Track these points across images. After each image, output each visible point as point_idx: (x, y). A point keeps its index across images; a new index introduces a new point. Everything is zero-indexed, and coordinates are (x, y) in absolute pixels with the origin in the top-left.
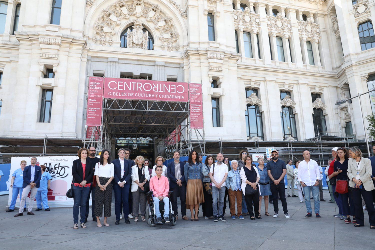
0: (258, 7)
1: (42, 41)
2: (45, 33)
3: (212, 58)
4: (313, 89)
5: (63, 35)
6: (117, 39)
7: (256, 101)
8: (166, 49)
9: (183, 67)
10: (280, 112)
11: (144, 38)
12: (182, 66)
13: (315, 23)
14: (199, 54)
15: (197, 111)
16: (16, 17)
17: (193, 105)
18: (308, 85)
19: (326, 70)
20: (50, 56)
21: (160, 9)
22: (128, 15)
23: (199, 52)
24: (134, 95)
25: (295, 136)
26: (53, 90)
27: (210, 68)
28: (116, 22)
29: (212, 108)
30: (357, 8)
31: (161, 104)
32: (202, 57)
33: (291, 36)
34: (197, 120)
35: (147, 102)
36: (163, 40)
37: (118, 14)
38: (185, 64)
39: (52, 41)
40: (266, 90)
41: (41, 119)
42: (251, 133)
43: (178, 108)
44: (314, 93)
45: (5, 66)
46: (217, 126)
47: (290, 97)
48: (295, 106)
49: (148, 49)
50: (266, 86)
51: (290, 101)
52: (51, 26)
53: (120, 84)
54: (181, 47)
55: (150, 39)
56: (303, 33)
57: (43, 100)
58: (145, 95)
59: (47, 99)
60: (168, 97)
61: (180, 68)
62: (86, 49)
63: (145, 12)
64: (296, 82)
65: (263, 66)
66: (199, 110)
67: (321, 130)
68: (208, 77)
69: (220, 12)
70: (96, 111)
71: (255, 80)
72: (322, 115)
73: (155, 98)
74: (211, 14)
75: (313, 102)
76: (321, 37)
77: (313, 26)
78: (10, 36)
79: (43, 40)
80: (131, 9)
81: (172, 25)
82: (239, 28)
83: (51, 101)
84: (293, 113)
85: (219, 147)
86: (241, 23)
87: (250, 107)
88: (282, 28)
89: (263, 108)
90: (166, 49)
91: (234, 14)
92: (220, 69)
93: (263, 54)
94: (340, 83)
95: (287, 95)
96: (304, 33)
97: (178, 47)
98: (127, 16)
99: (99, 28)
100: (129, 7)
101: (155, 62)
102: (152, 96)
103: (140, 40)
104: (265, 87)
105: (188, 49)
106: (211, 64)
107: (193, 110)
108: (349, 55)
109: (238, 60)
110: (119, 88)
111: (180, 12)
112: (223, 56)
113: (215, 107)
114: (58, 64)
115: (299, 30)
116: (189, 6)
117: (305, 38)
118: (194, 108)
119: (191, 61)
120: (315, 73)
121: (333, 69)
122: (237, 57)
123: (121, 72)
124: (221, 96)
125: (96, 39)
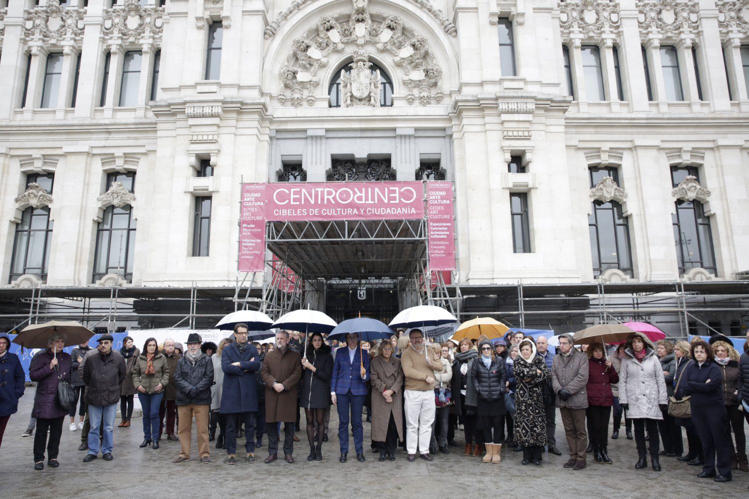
2: (195, 99)
3: (508, 112)
6: (322, 92)
8: (417, 102)
9: (451, 136)
10: (672, 214)
11: (373, 84)
15: (444, 237)
16: (155, 72)
17: (435, 224)
20: (205, 138)
21: (401, 23)
22: (342, 43)
23: (482, 102)
24: (320, 212)
25: (712, 265)
27: (505, 133)
28: (319, 60)
29: (513, 215)
31: (372, 225)
32: (486, 112)
33: (700, 41)
34: (443, 254)
35: (346, 223)
36: (410, 86)
37: (323, 45)
38: (454, 129)
39: (207, 111)
40: (637, 168)
43: (406, 232)
46: (525, 251)
47: (698, 180)
48: (708, 199)
49: (382, 106)
51: (696, 188)
52: (205, 84)
53: (295, 193)
55: (387, 85)
58: (341, 211)
60: (383, 212)
61: (444, 137)
63: (374, 33)
64: (710, 145)
65: (629, 116)
66: (446, 233)
69: (523, 15)
70: (254, 244)
73: (360, 215)
74: (506, 20)
79: (192, 112)
80: (347, 32)
82: (571, 40)
83: (209, 218)
84: (706, 215)
85: (518, 298)
86: (576, 28)
87: (602, 206)
88: (675, 25)
89: (631, 207)
90: (417, 102)
91: (559, 12)
92: (526, 134)
93: (629, 89)
95: (689, 174)
97: (441, 95)
98: (340, 46)
101: (394, 130)
102: (352, 212)
103: (365, 90)
105: (459, 98)
107: (434, 235)
110: (293, 202)
112: (531, 106)
113: (519, 211)
114: (219, 151)
118: (438, 231)
119: (465, 121)
123: (332, 155)
124: (530, 189)
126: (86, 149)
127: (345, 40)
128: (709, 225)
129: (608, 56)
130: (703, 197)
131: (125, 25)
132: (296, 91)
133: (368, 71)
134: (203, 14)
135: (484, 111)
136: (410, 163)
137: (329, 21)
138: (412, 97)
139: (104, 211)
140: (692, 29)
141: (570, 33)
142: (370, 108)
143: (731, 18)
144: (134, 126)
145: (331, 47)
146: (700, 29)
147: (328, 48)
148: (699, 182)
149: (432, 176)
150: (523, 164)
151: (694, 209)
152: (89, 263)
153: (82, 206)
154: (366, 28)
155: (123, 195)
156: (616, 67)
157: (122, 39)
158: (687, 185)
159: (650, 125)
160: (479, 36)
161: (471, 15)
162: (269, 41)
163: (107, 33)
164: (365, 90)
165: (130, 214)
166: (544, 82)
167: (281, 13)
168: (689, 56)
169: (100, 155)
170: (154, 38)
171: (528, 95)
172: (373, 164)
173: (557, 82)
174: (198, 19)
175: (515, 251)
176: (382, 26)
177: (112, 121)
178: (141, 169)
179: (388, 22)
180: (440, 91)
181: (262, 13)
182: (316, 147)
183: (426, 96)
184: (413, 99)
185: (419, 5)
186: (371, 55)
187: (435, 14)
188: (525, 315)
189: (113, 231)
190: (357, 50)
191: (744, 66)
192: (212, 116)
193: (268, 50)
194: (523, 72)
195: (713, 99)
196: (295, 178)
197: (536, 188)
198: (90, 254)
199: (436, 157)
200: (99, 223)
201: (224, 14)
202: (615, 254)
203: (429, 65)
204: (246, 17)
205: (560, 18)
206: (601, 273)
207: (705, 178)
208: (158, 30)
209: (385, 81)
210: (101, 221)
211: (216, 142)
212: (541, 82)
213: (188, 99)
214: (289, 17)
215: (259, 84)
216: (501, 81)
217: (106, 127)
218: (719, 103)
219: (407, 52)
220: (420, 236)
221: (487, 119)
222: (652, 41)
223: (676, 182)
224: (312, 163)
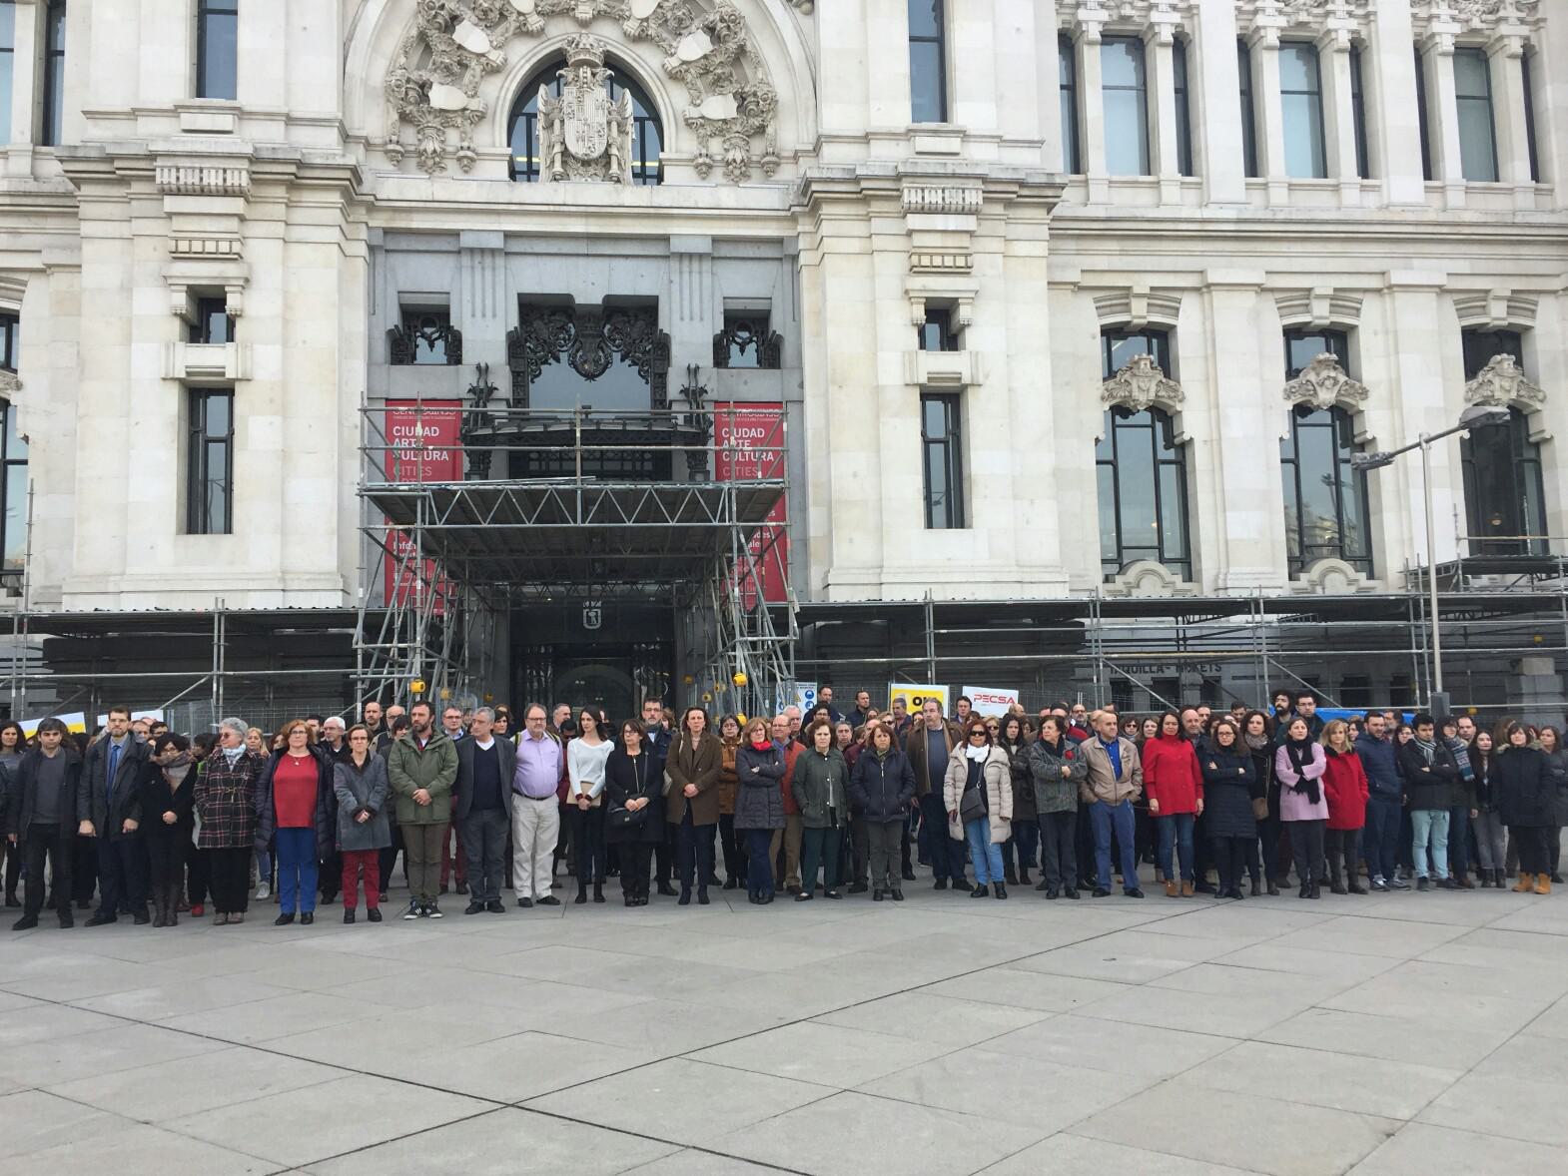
1: (169, 183)
3: (922, 211)
5: (256, 149)
6: (492, 137)
8: (718, 173)
9: (795, 258)
11: (614, 125)
12: (791, 251)
14: (864, 199)
20: (210, 247)
22: (539, 13)
23: (864, 184)
27: (915, 260)
28: (483, 55)
29: (927, 442)
32: (876, 206)
33: (1369, 35)
36: (702, 131)
37: (491, 15)
38: (801, 245)
39: (213, 179)
40: (1209, 335)
42: (1124, 544)
44: (1480, 331)
45: (27, 289)
48: (1362, 406)
54: (788, 158)
55: (650, 125)
56: (1434, 11)
59: (210, 434)
61: (781, 259)
64: (1375, 282)
65: (1198, 215)
68: (907, 302)
72: (1524, 441)
75: (1471, 372)
78: (34, 152)
79: (173, 181)
81: (742, 50)
83: (228, 441)
84: (1357, 440)
87: (1131, 420)
89: (1192, 424)
90: (718, 173)
92: (961, 262)
95: (1328, 350)
97: (774, 159)
99: (411, 93)
101: (665, 239)
103: (596, 140)
104: (1204, 318)
105: (814, 174)
106: (919, 240)
109: (1055, 204)
112: (974, 198)
113: (941, 435)
114: (247, 280)
117: (1446, 33)
119: (826, 228)
120: (1485, 224)
122: (1050, 192)
123: (520, 295)
125: (398, 148)
130: (1354, 402)
133: (601, 93)
135: (869, 206)
136: (702, 319)
138: (708, 161)
142: (609, 186)
145: (512, 23)
146: (1370, 8)
149: (751, 348)
150: (954, 328)
151: (1333, 426)
156: (1177, 91)
158: (1318, 375)
159: (1245, 235)
166: (1006, 137)
168: (1343, 72)
171: (970, 171)
173: (1036, 139)
175: (930, 525)
180: (770, 150)
183: (738, 161)
184: (710, 167)
186: (609, 48)
188: (937, 663)
192: (226, 193)
193: (354, 25)
194: (963, 113)
195: (1387, 175)
196: (432, 346)
197: (980, 385)
199: (760, 305)
202: (1155, 525)
206: (1121, 569)
207: (1359, 357)
209: (645, 114)
211: (237, 258)
212: (1000, 137)
213: (159, 146)
215: (340, 115)
216: (909, 134)
219: (694, 46)
221: (878, 225)
222: (1262, 32)
223: (1295, 366)
224: (473, 316)
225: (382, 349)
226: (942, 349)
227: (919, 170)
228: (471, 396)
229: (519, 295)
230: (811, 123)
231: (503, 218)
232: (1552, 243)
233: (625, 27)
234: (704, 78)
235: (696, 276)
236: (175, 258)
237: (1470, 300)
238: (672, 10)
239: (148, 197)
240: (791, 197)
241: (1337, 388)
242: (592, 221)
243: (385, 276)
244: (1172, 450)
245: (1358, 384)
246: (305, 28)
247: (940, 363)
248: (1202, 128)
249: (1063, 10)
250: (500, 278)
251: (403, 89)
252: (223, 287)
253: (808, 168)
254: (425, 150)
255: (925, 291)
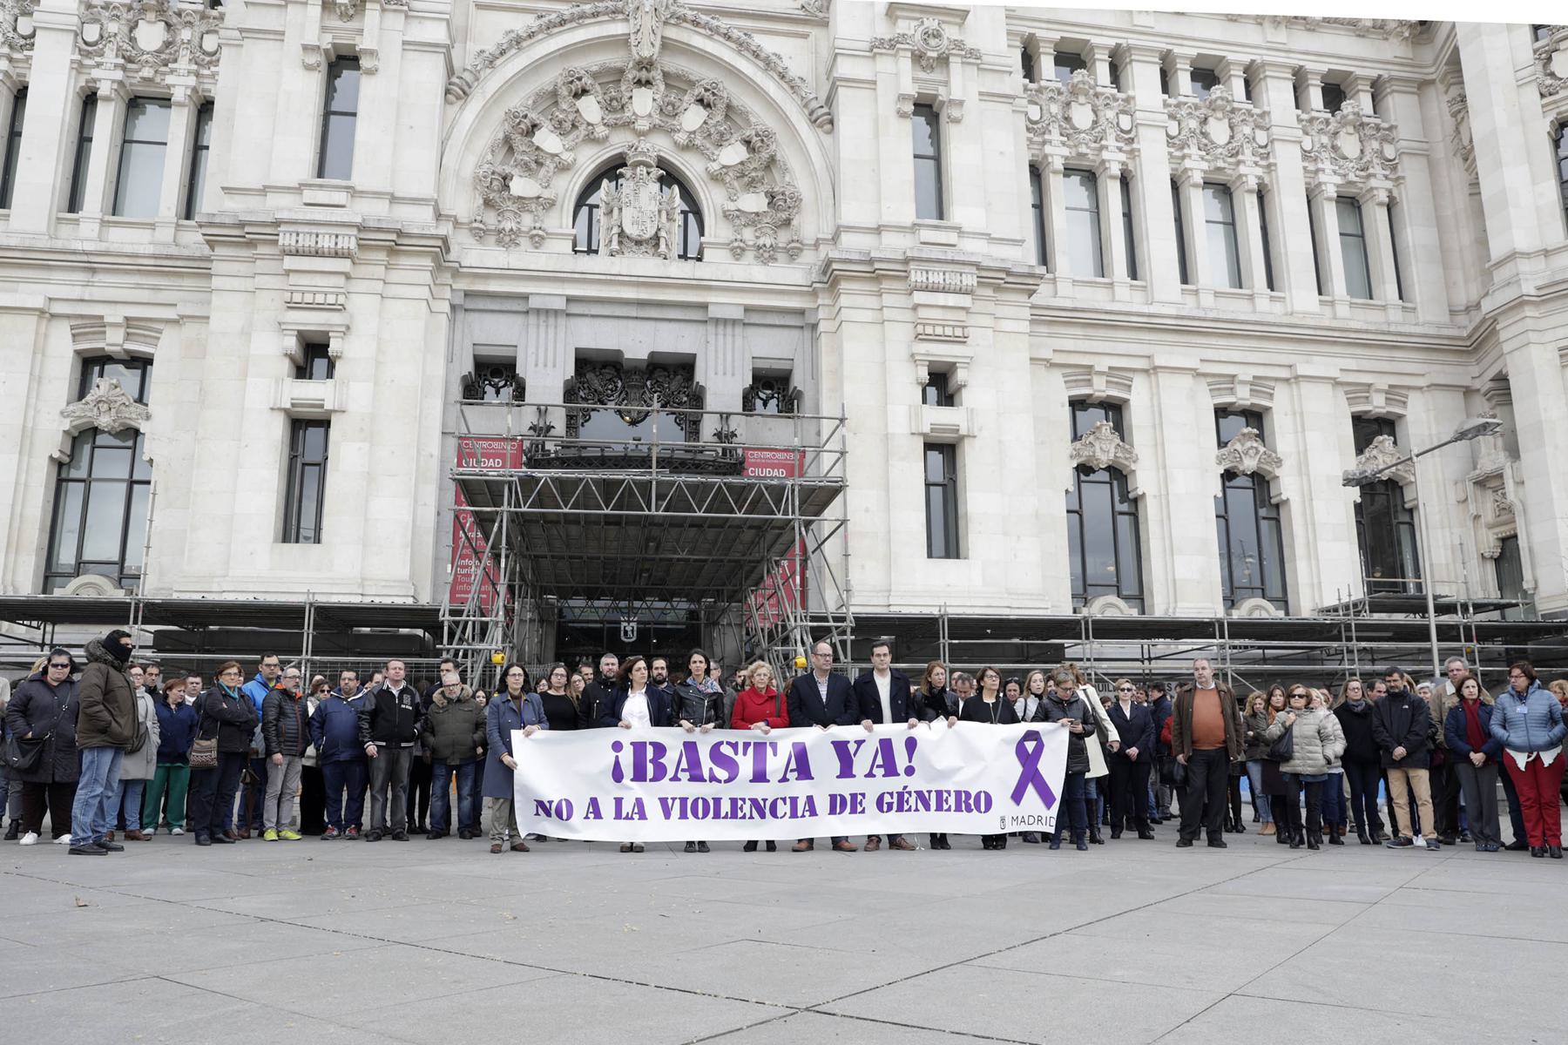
0: (1129, 66)
1: (290, 245)
2: (300, 216)
4: (1362, 400)
5: (364, 220)
6: (560, 221)
7: (1113, 450)
9: (814, 327)
11: (664, 214)
12: (813, 321)
13: (1378, 121)
14: (876, 277)
16: (198, 148)
18: (1336, 383)
19: (1421, 320)
20: (320, 298)
21: (725, 95)
22: (605, 124)
23: (877, 265)
26: (329, 422)
27: (920, 329)
28: (557, 155)
29: (928, 485)
30: (1550, 59)
32: (886, 285)
33: (1271, 181)
36: (737, 222)
38: (821, 314)
39: (326, 243)
40: (1156, 409)
41: (290, 531)
42: (1089, 582)
44: (1366, 417)
45: (162, 336)
46: (947, 556)
47: (1261, 436)
48: (1277, 472)
49: (680, 257)
50: (1155, 390)
51: (1257, 452)
52: (321, 186)
54: (810, 245)
55: (691, 216)
56: (1320, 166)
57: (293, 459)
59: (308, 459)
61: (802, 327)
62: (447, 264)
63: (669, 111)
64: (1284, 373)
65: (1146, 309)
67: (1396, 569)
68: (913, 365)
69: (961, 103)
71: (1110, 368)
72: (1399, 508)
76: (1403, 178)
77: (1369, 132)
78: (178, 225)
79: (293, 243)
80: (615, 103)
81: (772, 160)
82: (1046, 156)
83: (322, 465)
84: (1273, 501)
87: (1092, 477)
88: (1230, 146)
89: (1144, 481)
91: (1025, 102)
92: (958, 332)
94: (1477, 374)
95: (1247, 426)
96: (1327, 166)
99: (495, 183)
100: (605, 94)
101: (704, 307)
103: (648, 225)
104: (1152, 394)
105: (834, 254)
106: (923, 313)
108: (1512, 256)
109: (1035, 291)
111: (806, 106)
112: (970, 280)
113: (940, 479)
114: (348, 328)
115: (1306, 155)
116: (838, 83)
117: (1331, 184)
119: (844, 300)
120: (1366, 331)
121: (1452, 313)
123: (577, 350)
124: (962, 438)
125: (481, 226)
126: (39, 303)
127: (611, 118)
128: (1277, 520)
129: (1112, 193)
130: (1270, 469)
131: (132, 40)
132: (508, 214)
134: (319, 40)
135: (881, 284)
136: (733, 375)
137: (579, 79)
138: (742, 245)
139: (74, 439)
140: (1258, 159)
141: (1044, 143)
142: (659, 261)
143: (1323, 146)
144: (152, 262)
147: (575, 133)
148: (1263, 441)
149: (773, 402)
150: (951, 388)
151: (1254, 489)
152: (39, 549)
153: (24, 427)
154: (654, 100)
155: (123, 408)
156: (1124, 215)
157: (124, 69)
158: (1243, 445)
159: (1183, 329)
160: (877, 136)
161: (864, 94)
162: (456, 107)
163: (89, 53)
164: (648, 225)
165: (134, 448)
167: (482, 51)
169: (68, 317)
170: (197, 75)
172: (657, 373)
173: (1018, 238)
174: (305, 48)
175: (930, 556)
176: (686, 98)
177: (102, 247)
178: (166, 352)
179: (699, 91)
180: (795, 238)
181: (444, 50)
182: (547, 332)
183: (768, 246)
184: (743, 250)
185: (761, 64)
186: (662, 154)
187: (793, 86)
189: (93, 484)
190: (635, 142)
191: (1341, 234)
192: (336, 255)
193: (452, 127)
194: (959, 212)
196: (498, 393)
197: (974, 437)
198: (41, 530)
200: (60, 465)
201: (363, 43)
202: (1112, 569)
203: (776, 184)
204: (411, 55)
205: (1026, 114)
206: (1086, 603)
207: (1273, 433)
208: (208, 59)
210: (67, 460)
211: (341, 309)
213: (284, 215)
214: (498, 62)
216: (915, 228)
217: (85, 258)
218: (1301, 296)
219: (733, 154)
220: (785, 513)
221: (888, 299)
222: (1190, 173)
224: (536, 365)
225: (457, 391)
226: (938, 405)
227: (924, 255)
228: (532, 432)
229: (576, 349)
230: (830, 217)
231: (566, 285)
232: (1418, 349)
233: (676, 137)
234: (740, 180)
235: (729, 339)
236: (289, 307)
237: (1357, 391)
238: (715, 126)
239: (271, 258)
240: (813, 275)
241: (1258, 456)
242: (642, 290)
243: (463, 332)
244: (1126, 504)
245: (1274, 455)
246: (411, 127)
247: (939, 417)
248: (1145, 243)
249: (1031, 146)
250: (561, 335)
251: (489, 179)
252: (328, 332)
253: (826, 251)
254: (504, 229)
255: (928, 355)
